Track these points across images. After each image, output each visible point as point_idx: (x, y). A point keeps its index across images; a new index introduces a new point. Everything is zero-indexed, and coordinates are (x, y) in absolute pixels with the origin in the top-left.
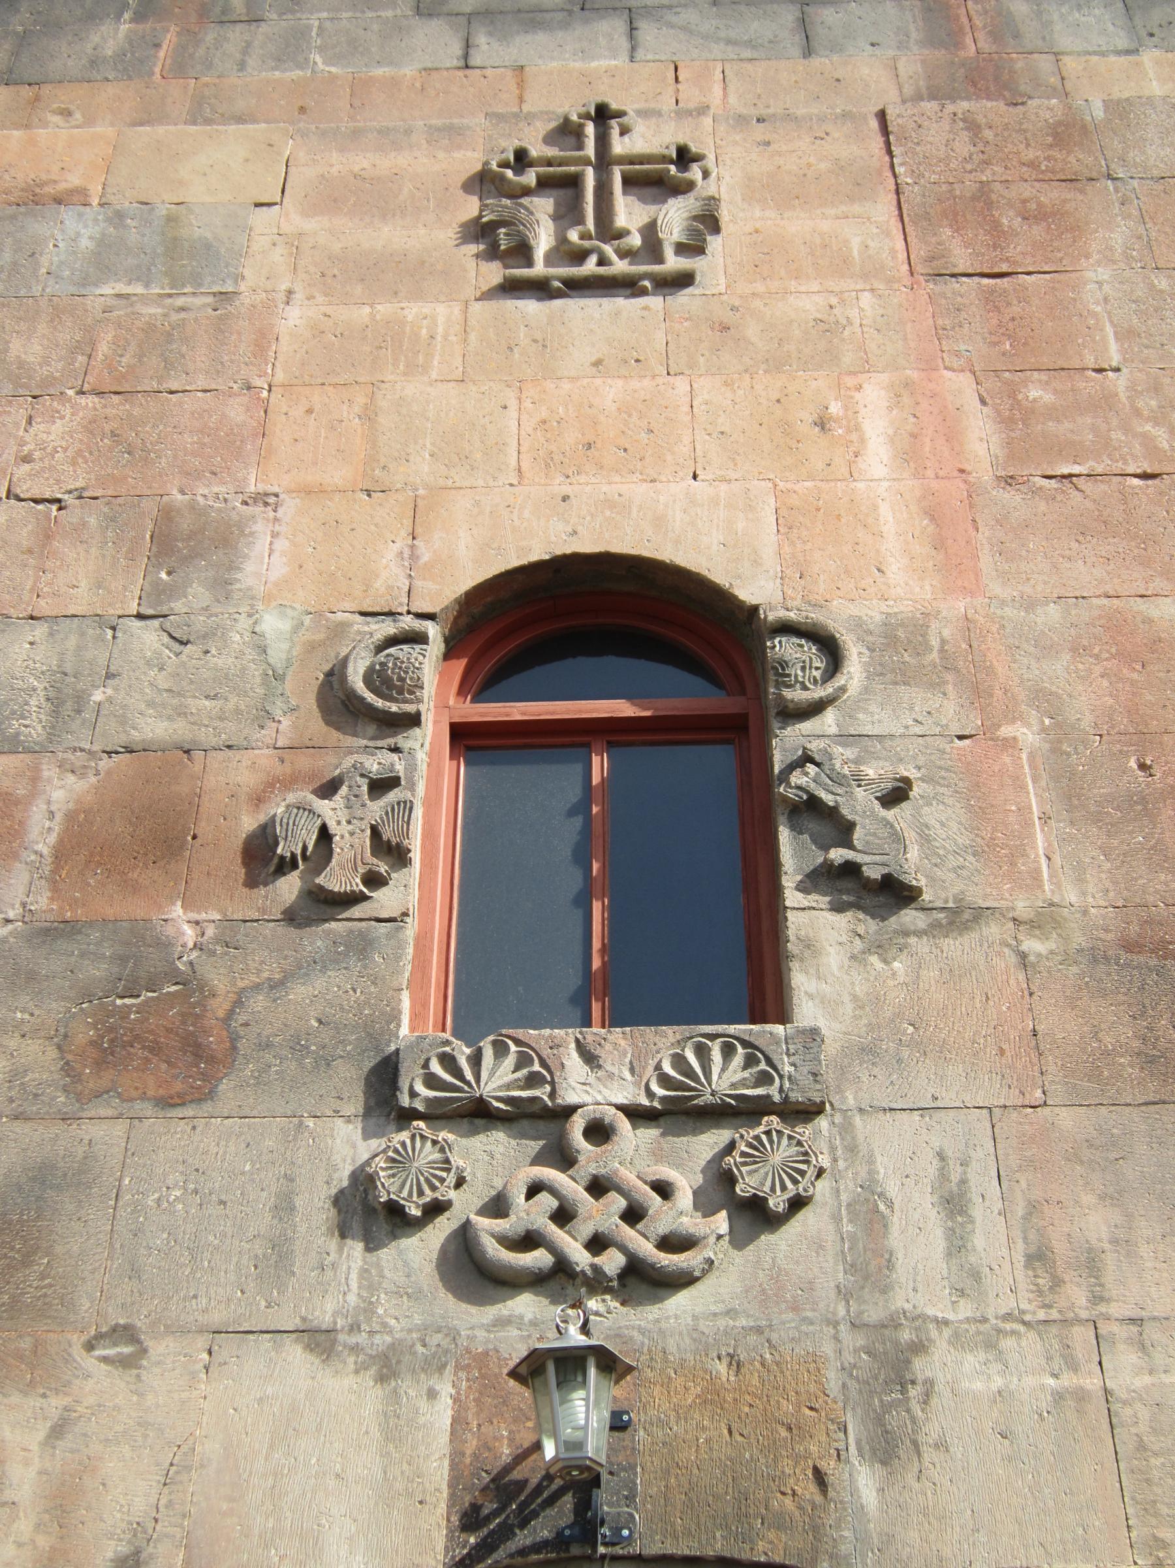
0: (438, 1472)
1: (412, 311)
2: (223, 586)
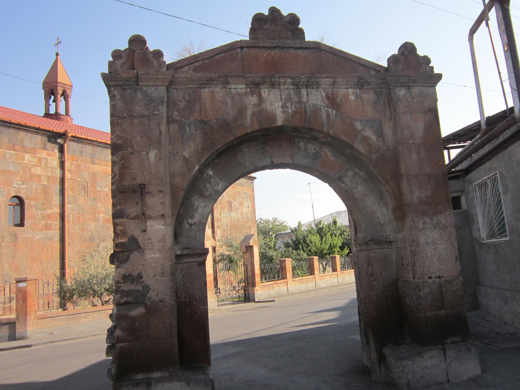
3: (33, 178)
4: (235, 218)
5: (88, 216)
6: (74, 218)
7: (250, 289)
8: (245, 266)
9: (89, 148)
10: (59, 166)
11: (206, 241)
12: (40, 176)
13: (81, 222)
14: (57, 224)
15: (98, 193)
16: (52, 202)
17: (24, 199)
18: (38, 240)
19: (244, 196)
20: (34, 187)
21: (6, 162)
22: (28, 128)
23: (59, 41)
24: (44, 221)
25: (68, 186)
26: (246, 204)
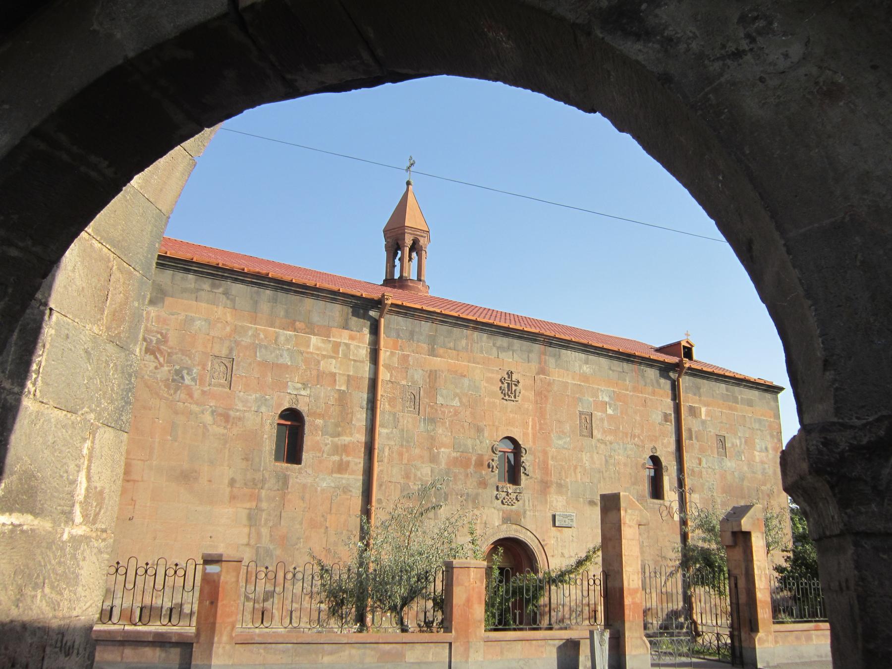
1: (496, 400)
2: (483, 436)
3: (322, 377)
4: (733, 472)
5: (417, 451)
6: (392, 452)
7: (744, 636)
8: (732, 579)
9: (426, 327)
10: (368, 359)
11: (626, 511)
12: (333, 375)
13: (405, 461)
14: (358, 462)
15: (439, 409)
16: (353, 423)
17: (304, 414)
18: (323, 490)
20: (322, 395)
21: (279, 349)
22: (318, 292)
23: (412, 161)
24: (336, 456)
26: (759, 443)
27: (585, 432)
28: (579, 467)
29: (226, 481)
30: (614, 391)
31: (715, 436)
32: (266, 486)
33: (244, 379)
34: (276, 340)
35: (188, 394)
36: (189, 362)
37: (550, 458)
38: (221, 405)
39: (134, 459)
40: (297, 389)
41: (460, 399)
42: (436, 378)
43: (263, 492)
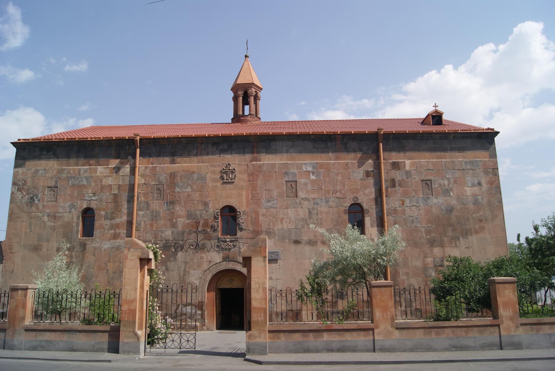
0: (222, 257)
2: (208, 208)
5: (162, 222)
6: (146, 225)
13: (154, 229)
15: (177, 195)
18: (105, 250)
19: (469, 167)
20: (104, 198)
25: (141, 192)
27: (291, 195)
28: (285, 219)
29: (55, 249)
30: (316, 163)
31: (420, 183)
32: (75, 250)
33: (63, 196)
34: (79, 173)
35: (36, 208)
36: (37, 192)
37: (260, 215)
38: (52, 211)
39: (13, 243)
40: (91, 197)
41: (191, 187)
42: (174, 177)
43: (74, 253)
